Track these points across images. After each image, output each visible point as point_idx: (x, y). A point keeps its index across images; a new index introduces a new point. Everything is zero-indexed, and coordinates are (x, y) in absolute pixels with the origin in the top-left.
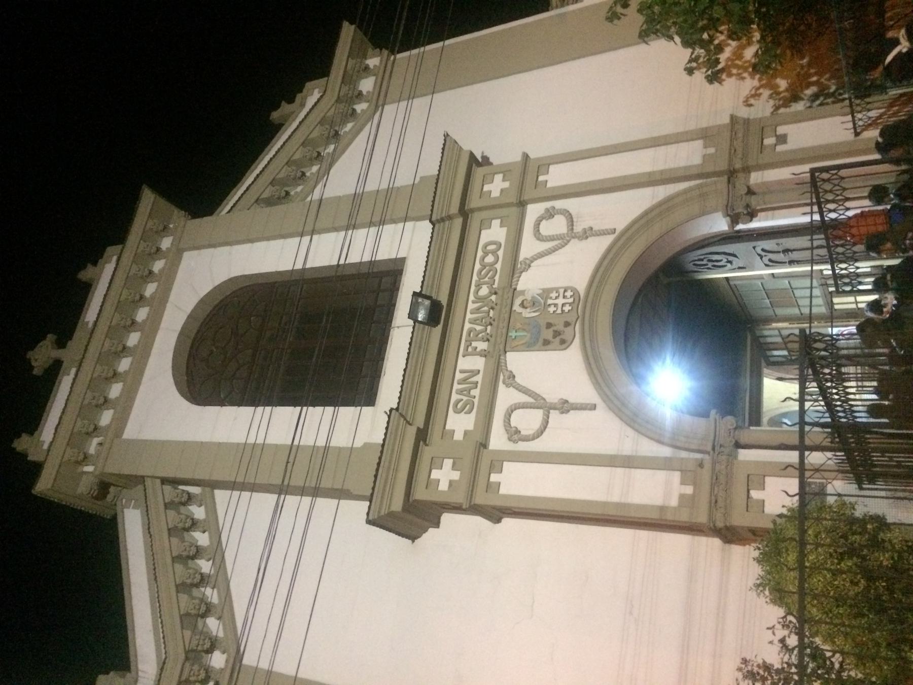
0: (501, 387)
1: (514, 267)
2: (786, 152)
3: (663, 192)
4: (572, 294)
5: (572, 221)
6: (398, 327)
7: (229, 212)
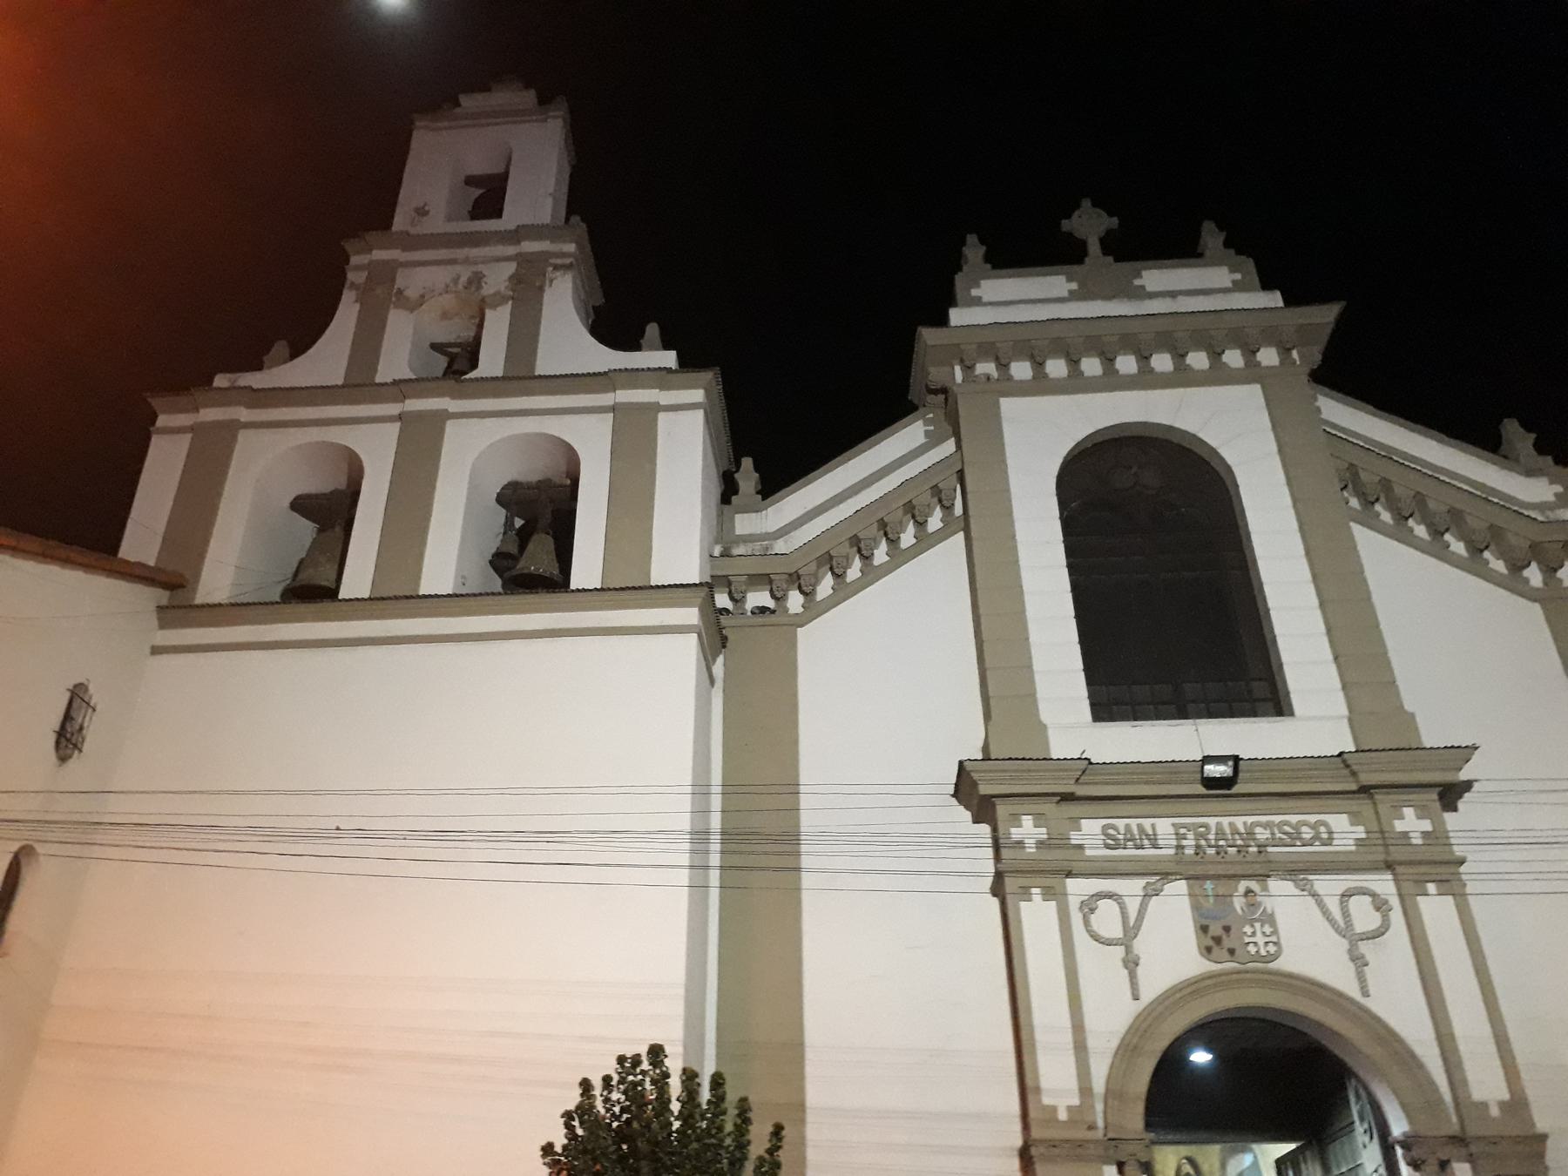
1: (1298, 871)
4: (1272, 952)
5: (1374, 938)
6: (1197, 730)
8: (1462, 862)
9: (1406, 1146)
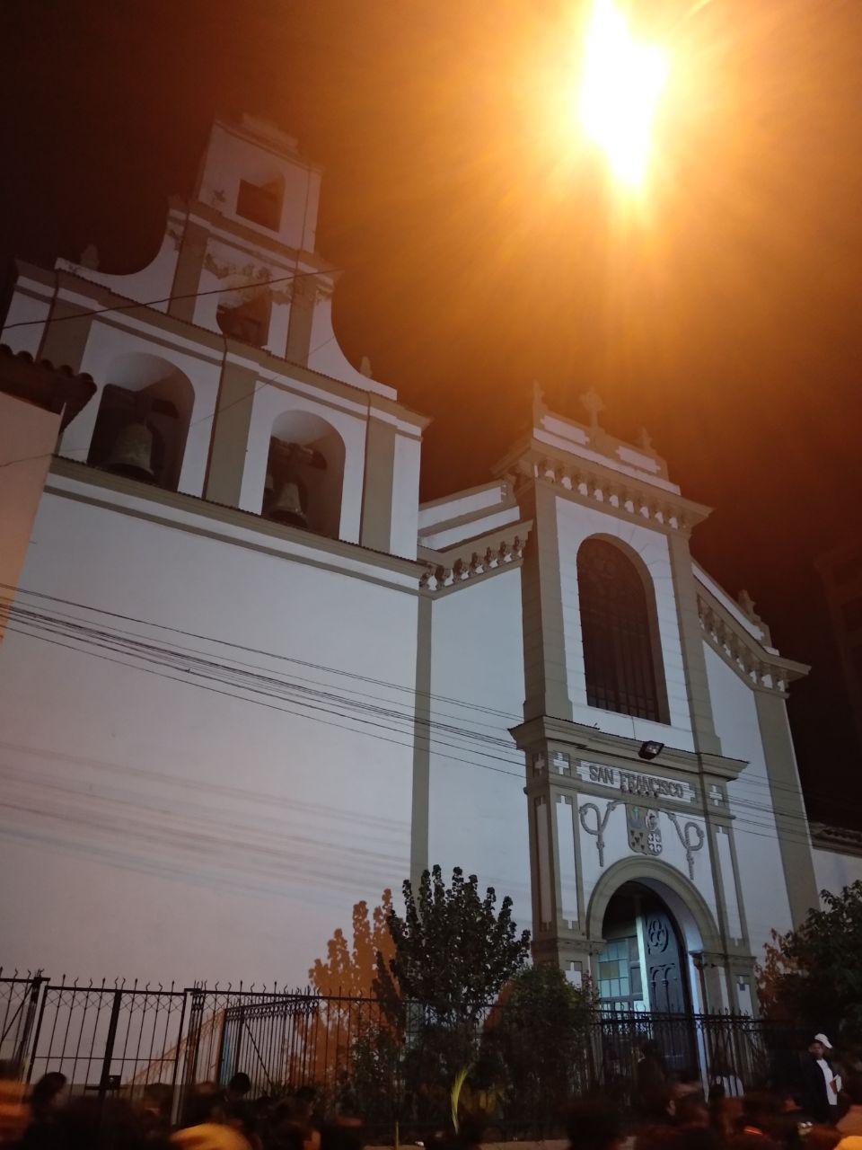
0: (606, 801)
1: (672, 808)
2: (736, 988)
3: (714, 911)
7: (696, 578)
8: (734, 818)
9: (696, 956)
